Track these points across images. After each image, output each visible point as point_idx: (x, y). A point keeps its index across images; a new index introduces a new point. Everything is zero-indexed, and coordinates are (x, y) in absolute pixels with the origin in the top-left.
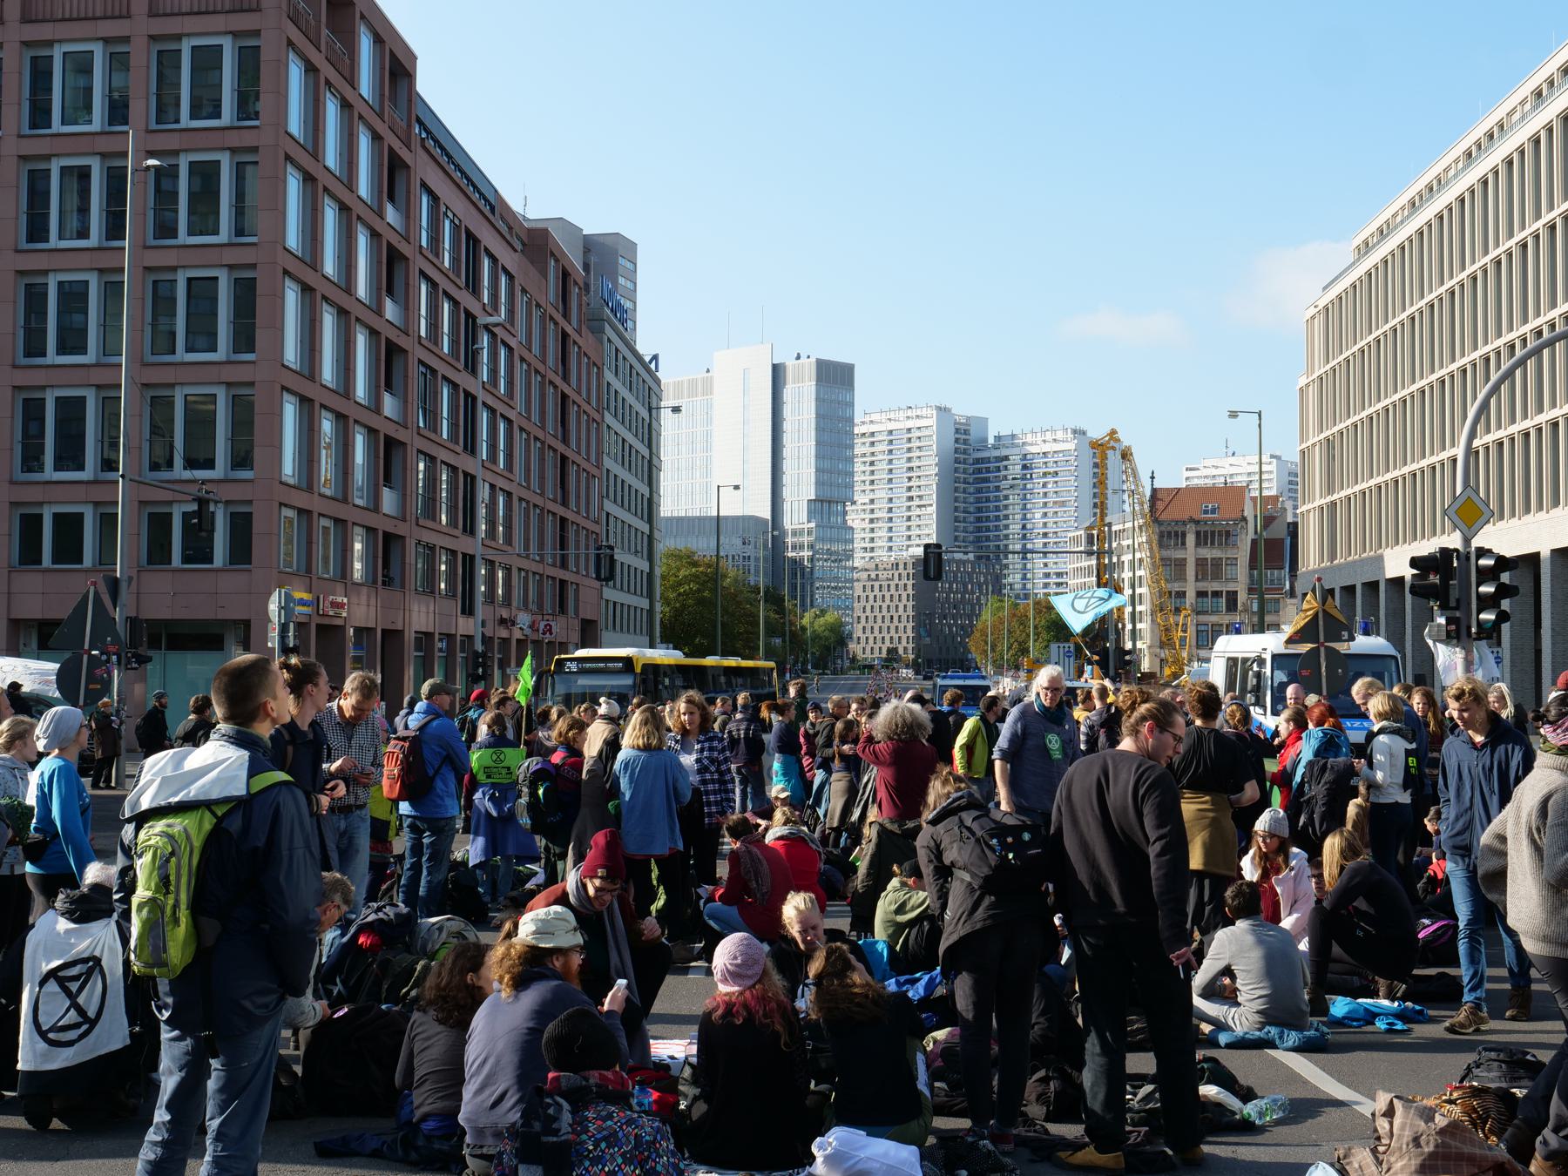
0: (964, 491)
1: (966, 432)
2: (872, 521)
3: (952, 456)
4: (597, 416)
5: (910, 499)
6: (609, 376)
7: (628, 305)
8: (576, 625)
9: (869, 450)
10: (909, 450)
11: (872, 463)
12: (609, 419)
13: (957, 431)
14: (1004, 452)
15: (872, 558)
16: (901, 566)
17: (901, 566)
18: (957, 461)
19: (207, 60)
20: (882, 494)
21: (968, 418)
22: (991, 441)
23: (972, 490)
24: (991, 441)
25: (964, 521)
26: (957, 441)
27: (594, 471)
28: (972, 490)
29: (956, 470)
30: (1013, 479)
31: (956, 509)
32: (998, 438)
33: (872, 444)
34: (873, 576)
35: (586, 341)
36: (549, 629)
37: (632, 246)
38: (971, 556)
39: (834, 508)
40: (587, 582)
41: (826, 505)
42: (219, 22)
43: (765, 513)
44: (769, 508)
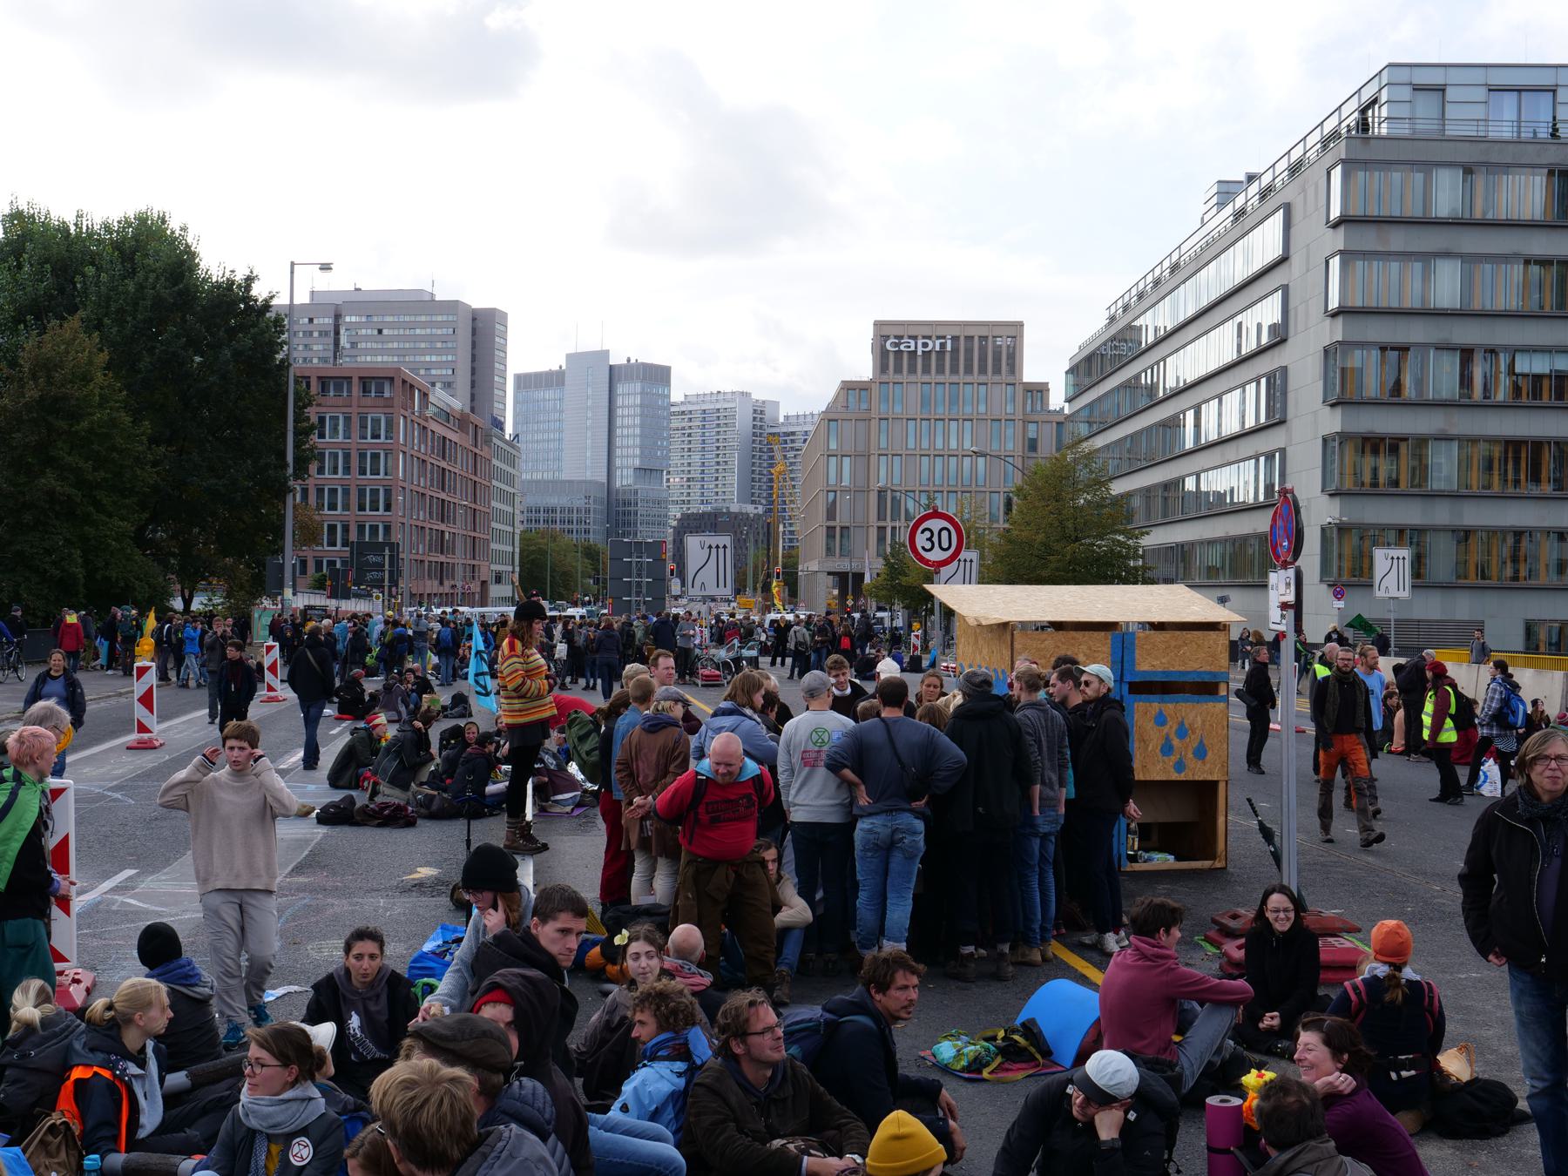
0: (760, 458)
1: (762, 412)
2: (688, 480)
3: (750, 430)
4: (488, 484)
5: (718, 463)
6: (495, 462)
7: (502, 419)
8: (479, 583)
9: (686, 424)
10: (718, 425)
11: (689, 435)
12: (494, 483)
13: (755, 411)
14: (791, 429)
15: (689, 509)
16: (706, 517)
17: (706, 517)
18: (754, 434)
19: (376, 422)
20: (696, 458)
21: (764, 402)
22: (781, 420)
23: (765, 458)
24: (781, 420)
25: (760, 481)
26: (755, 419)
27: (488, 510)
28: (765, 458)
29: (754, 441)
30: (798, 450)
31: (753, 471)
32: (787, 417)
33: (690, 419)
34: (686, 524)
35: (483, 452)
36: (470, 588)
37: (504, 316)
38: (761, 510)
39: (654, 473)
40: (483, 563)
41: (648, 472)
42: (380, 410)
43: (604, 479)
44: (606, 474)
